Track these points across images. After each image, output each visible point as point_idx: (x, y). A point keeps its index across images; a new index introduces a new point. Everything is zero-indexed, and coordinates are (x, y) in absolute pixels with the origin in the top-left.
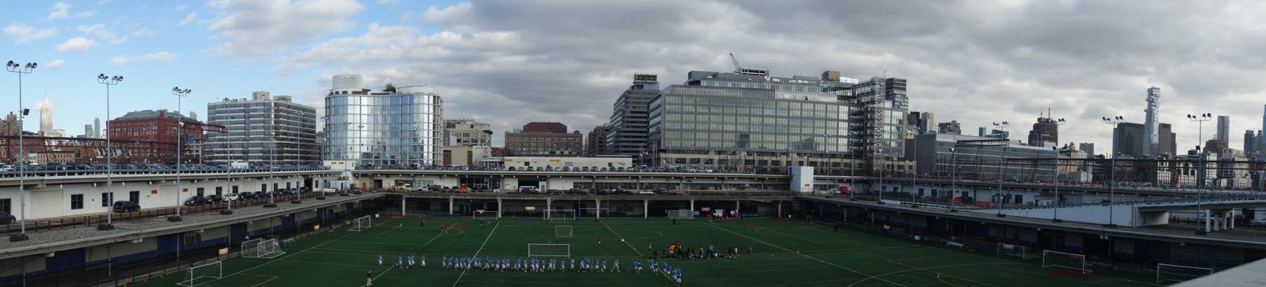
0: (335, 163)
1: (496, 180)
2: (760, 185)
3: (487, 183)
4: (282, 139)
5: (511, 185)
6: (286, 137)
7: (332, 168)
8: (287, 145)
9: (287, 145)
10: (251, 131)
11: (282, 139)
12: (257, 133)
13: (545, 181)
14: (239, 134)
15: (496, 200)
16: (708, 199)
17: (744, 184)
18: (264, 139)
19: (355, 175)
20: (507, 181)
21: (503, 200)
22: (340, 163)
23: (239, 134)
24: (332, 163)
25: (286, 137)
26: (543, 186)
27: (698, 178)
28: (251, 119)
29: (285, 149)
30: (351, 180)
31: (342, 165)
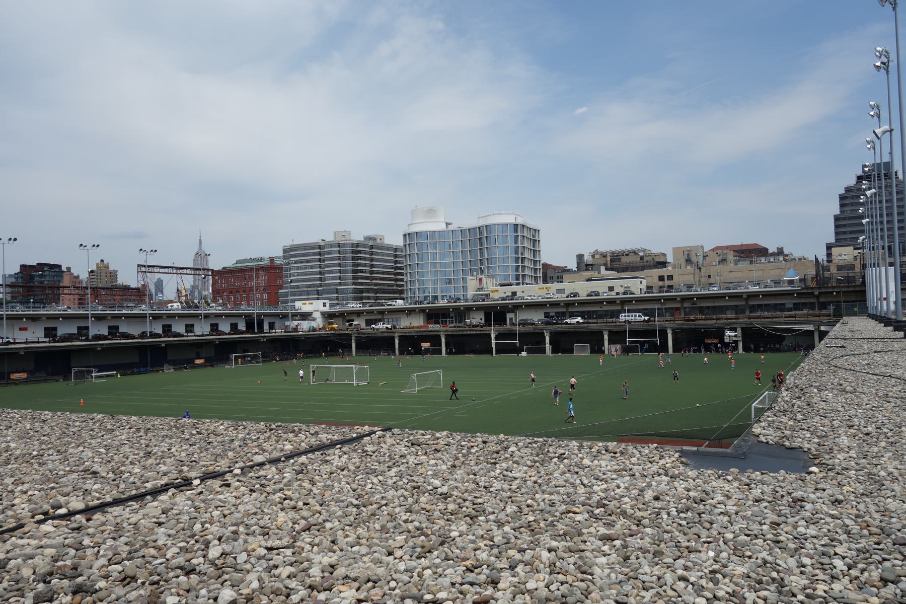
0: (306, 304)
1: (461, 313)
2: (814, 303)
3: (452, 318)
4: (362, 284)
5: (477, 318)
6: (369, 281)
7: (302, 309)
8: (368, 291)
9: (368, 291)
10: (326, 275)
11: (362, 284)
12: (333, 278)
13: (513, 312)
14: (315, 280)
15: (440, 336)
16: (693, 327)
17: (784, 304)
18: (340, 284)
19: (323, 314)
20: (472, 315)
21: (446, 336)
22: (309, 304)
23: (315, 280)
24: (303, 304)
25: (369, 281)
26: (511, 319)
27: (701, 298)
28: (326, 263)
29: (364, 295)
30: (319, 322)
31: (310, 305)
